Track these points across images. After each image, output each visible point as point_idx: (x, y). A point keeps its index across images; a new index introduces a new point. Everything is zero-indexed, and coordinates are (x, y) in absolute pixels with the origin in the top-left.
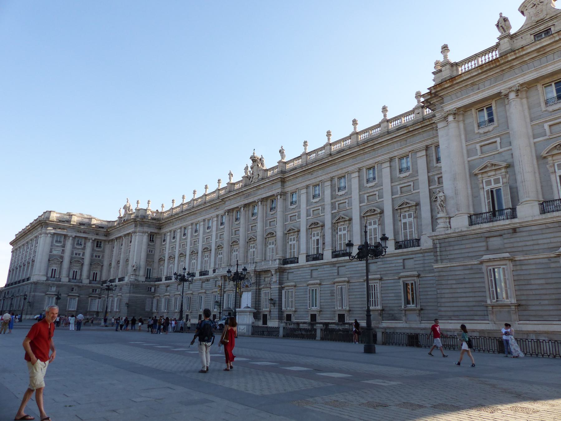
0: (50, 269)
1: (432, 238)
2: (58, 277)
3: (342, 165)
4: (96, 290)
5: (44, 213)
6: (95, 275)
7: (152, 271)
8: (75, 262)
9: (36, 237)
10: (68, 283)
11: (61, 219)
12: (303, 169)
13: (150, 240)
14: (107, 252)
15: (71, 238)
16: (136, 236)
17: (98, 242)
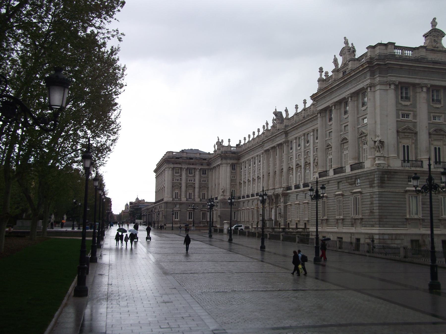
0: (174, 192)
2: (179, 198)
3: (304, 128)
4: (205, 206)
5: (167, 153)
6: (204, 195)
7: (236, 192)
8: (189, 186)
9: (164, 170)
10: (187, 202)
11: (177, 157)
13: (233, 169)
14: (210, 177)
15: (185, 170)
16: (222, 166)
17: (203, 170)
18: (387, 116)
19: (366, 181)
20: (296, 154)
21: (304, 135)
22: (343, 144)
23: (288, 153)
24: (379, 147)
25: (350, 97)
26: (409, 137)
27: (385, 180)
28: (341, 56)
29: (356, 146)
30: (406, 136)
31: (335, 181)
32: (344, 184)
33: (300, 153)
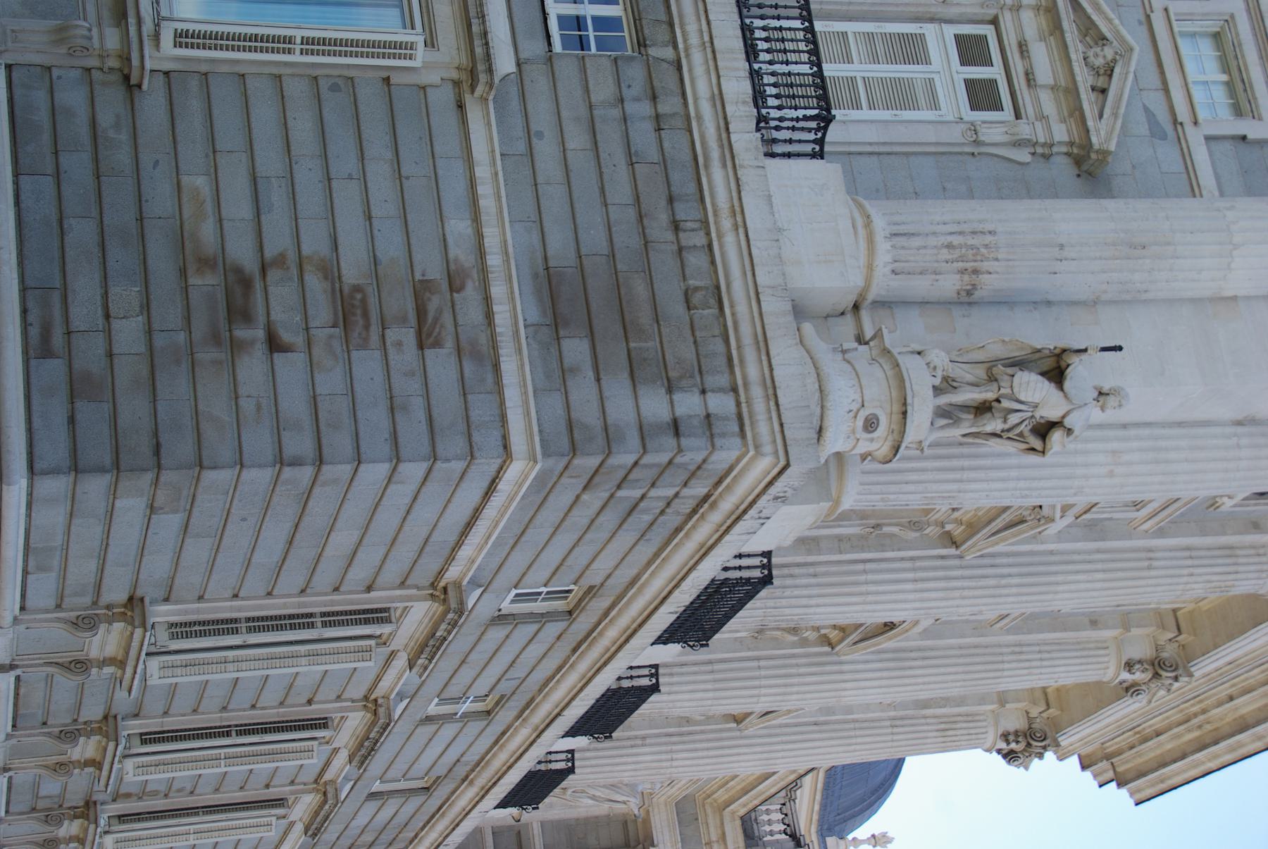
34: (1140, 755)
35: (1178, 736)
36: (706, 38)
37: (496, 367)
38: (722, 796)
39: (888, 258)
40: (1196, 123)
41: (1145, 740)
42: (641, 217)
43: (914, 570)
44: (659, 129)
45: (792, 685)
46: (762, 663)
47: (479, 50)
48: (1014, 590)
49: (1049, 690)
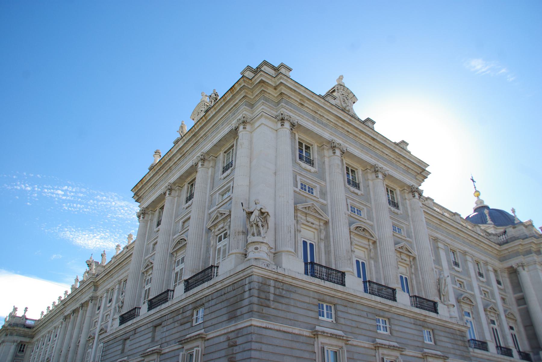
1: (102, 341)
12: (105, 272)
18: (275, 173)
19: (219, 306)
20: (103, 315)
21: (120, 282)
22: (177, 254)
23: (93, 315)
24: (257, 225)
25: (202, 159)
26: (314, 226)
27: (269, 300)
28: (193, 119)
29: (203, 246)
30: (309, 224)
31: (149, 325)
32: (165, 329)
33: (108, 311)
34: (414, 168)
35: (404, 162)
36: (201, 292)
37: (240, 329)
38: (495, 252)
39: (235, 250)
40: (230, 196)
41: (409, 168)
42: (223, 301)
43: (335, 229)
44: (213, 299)
45: (386, 248)
46: (382, 256)
47: (197, 337)
48: (338, 207)
49: (401, 190)
